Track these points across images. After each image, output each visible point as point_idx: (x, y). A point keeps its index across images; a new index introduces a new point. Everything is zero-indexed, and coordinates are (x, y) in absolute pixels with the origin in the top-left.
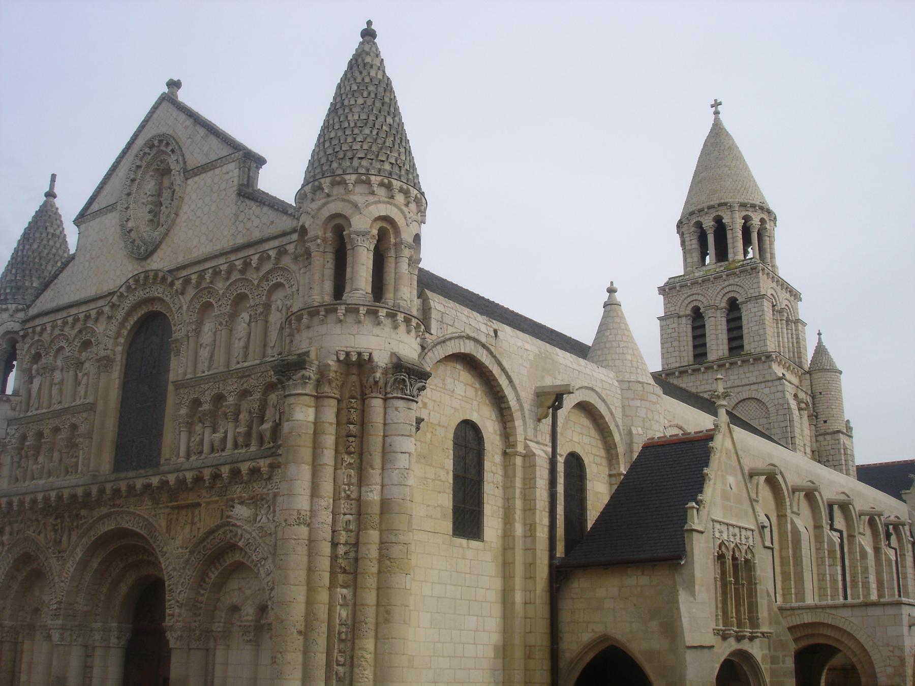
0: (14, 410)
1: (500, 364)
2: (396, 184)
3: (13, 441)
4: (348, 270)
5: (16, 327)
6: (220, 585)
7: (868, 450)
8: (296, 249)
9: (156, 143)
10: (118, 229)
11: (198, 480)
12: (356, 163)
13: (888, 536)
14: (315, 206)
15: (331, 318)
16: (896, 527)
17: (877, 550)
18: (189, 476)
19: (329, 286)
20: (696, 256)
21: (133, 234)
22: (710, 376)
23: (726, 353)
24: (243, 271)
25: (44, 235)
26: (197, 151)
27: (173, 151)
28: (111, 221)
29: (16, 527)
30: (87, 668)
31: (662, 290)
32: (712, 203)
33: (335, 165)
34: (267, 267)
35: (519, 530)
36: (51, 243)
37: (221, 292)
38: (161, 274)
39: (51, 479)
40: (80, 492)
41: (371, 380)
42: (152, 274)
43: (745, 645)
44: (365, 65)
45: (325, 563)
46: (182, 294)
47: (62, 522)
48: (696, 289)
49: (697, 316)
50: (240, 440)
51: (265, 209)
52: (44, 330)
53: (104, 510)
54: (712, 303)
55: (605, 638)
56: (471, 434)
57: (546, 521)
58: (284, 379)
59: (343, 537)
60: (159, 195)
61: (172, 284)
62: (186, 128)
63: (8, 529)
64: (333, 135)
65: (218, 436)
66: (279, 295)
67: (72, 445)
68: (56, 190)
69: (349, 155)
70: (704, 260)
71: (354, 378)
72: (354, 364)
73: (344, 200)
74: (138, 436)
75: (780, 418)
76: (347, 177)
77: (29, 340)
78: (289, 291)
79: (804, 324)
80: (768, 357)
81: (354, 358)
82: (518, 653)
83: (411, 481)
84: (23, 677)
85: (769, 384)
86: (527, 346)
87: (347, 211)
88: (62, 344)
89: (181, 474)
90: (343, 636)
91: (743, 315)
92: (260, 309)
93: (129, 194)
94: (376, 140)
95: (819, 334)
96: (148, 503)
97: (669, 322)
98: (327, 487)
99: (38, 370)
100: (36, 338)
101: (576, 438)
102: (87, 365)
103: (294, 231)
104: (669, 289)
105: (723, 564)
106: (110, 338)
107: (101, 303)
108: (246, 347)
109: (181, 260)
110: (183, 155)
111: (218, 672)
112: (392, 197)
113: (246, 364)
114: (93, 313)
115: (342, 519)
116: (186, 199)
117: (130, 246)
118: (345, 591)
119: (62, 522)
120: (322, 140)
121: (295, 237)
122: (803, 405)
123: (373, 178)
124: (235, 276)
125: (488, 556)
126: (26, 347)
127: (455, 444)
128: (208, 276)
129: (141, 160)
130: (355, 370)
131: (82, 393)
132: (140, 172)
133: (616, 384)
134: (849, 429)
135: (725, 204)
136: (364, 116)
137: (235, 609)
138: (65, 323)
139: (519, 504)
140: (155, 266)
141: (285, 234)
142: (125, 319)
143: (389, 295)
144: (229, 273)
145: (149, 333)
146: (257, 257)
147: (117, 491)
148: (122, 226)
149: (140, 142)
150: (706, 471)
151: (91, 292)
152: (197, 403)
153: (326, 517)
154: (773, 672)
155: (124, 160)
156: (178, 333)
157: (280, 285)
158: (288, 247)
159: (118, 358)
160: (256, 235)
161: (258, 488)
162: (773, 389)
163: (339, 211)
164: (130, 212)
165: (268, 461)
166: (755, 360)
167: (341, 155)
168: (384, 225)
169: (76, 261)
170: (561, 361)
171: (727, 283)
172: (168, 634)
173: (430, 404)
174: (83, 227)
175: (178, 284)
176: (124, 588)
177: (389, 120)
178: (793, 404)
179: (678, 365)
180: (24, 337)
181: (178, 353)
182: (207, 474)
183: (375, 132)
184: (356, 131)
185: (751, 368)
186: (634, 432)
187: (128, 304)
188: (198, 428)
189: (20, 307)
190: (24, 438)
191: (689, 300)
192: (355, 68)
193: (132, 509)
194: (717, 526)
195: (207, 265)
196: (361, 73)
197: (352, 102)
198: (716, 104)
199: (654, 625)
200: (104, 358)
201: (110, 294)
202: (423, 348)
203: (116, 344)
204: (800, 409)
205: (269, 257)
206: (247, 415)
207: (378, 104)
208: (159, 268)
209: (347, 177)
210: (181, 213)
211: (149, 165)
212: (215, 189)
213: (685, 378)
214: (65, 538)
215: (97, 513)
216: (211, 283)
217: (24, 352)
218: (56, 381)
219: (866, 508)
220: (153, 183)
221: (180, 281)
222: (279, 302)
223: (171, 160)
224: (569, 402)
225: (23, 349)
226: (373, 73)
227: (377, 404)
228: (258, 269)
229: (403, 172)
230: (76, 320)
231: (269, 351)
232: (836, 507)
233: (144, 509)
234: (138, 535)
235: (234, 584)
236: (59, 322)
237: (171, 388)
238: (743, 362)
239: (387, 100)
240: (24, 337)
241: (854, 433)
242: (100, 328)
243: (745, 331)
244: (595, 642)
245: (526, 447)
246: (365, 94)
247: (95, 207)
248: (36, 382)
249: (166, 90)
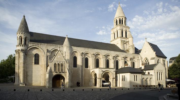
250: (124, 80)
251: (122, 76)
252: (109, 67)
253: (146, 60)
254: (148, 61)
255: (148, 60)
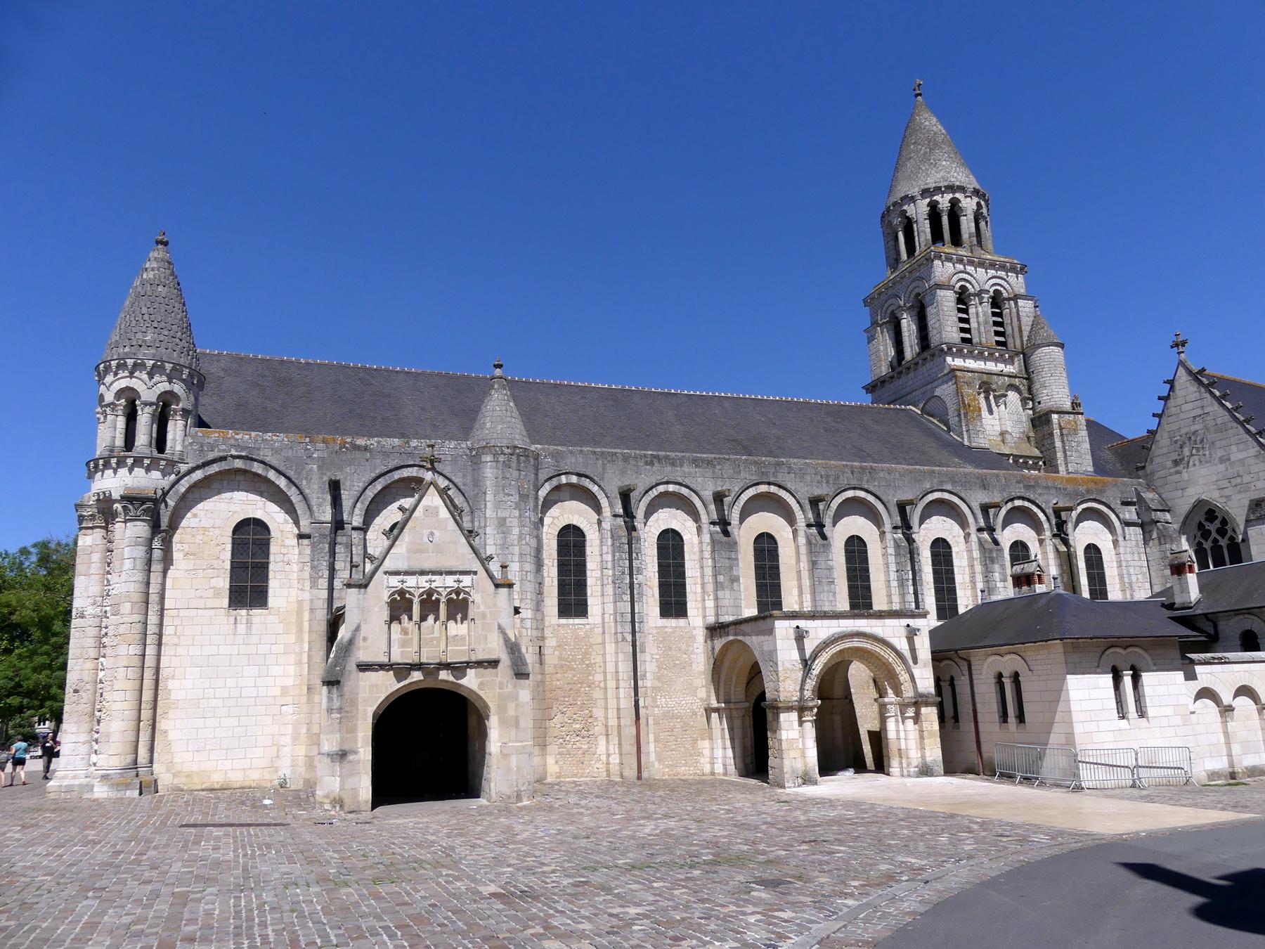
250: (1021, 718)
251: (1000, 676)
252: (870, 606)
253: (1208, 526)
254: (1222, 532)
255: (1224, 522)
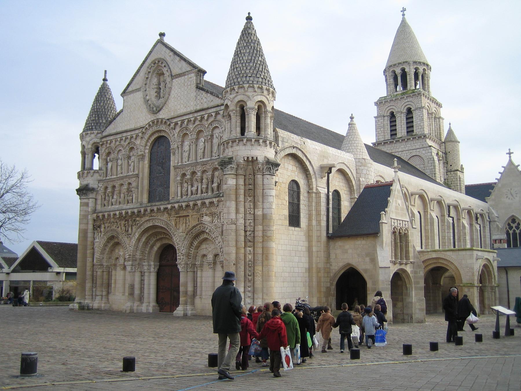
0: (101, 176)
1: (306, 156)
2: (264, 87)
3: (102, 189)
4: (246, 123)
5: (98, 140)
6: (198, 247)
7: (471, 178)
8: (224, 113)
9: (157, 62)
10: (142, 99)
11: (188, 206)
12: (248, 79)
13: (477, 219)
14: (232, 96)
15: (241, 143)
16: (481, 215)
17: (471, 225)
18: (184, 204)
19: (239, 129)
20: (393, 86)
21: (149, 102)
22: (398, 144)
23: (406, 134)
24: (201, 121)
25: (105, 99)
26: (177, 67)
27: (165, 66)
28: (139, 95)
29: (107, 225)
30: (142, 281)
31: (376, 104)
32: (400, 61)
33: (239, 80)
34: (211, 119)
35: (314, 223)
36: (108, 102)
37: (192, 129)
38: (164, 121)
39: (121, 205)
40: (136, 211)
41: (257, 167)
42: (160, 120)
43: (403, 267)
44: (249, 34)
45: (242, 238)
46: (174, 129)
47: (128, 223)
48: (392, 103)
49: (392, 115)
50: (204, 190)
51: (209, 95)
52: (111, 142)
53: (147, 218)
54: (399, 110)
55: (348, 264)
56: (295, 186)
57: (325, 218)
58: (223, 168)
59: (248, 228)
60: (159, 84)
61: (169, 125)
62: (170, 56)
63: (103, 226)
64: (237, 66)
65: (194, 188)
66: (217, 131)
67: (129, 191)
68: (107, 78)
69: (245, 75)
70: (396, 88)
71: (250, 167)
72: (250, 161)
73: (243, 95)
74: (158, 188)
75: (430, 165)
76: (245, 85)
77: (104, 146)
78: (221, 130)
79: (443, 119)
80: (425, 136)
81: (250, 159)
82: (314, 270)
83: (274, 207)
84: (113, 285)
85: (425, 149)
86: (317, 148)
87: (245, 99)
88: (120, 149)
89: (180, 204)
90: (250, 265)
91: (414, 116)
92: (209, 137)
93: (146, 84)
94: (255, 68)
95: (450, 124)
96: (166, 215)
97: (379, 119)
98: (242, 210)
99: (110, 159)
100: (108, 146)
101: (337, 184)
102: (133, 158)
103: (222, 105)
104: (380, 103)
105: (395, 236)
106: (143, 146)
107: (137, 132)
108: (204, 152)
109: (172, 115)
110: (170, 68)
111: (199, 280)
112: (263, 92)
113: (204, 160)
114: (134, 136)
115: (248, 222)
116: (173, 88)
117: (149, 107)
118: (250, 249)
119: (128, 223)
120: (233, 68)
121: (223, 107)
122: (441, 158)
123: (255, 85)
124: (197, 123)
125: (302, 234)
126: (103, 149)
127: (289, 190)
128: (185, 123)
129: (150, 69)
130: (251, 164)
131: (132, 169)
132: (150, 75)
133: (354, 160)
134: (462, 168)
135: (406, 62)
136: (250, 58)
137: (204, 256)
138: (121, 140)
139: (314, 213)
140: (161, 117)
141: (218, 106)
142: (149, 139)
143: (262, 133)
144: (195, 121)
145: (160, 145)
146: (207, 115)
147: (152, 211)
148: (144, 98)
149: (149, 61)
150: (389, 199)
151: (132, 127)
152: (184, 175)
153: (242, 221)
154: (415, 277)
155: (142, 68)
156: (173, 146)
157: (216, 127)
158: (220, 112)
159: (147, 155)
160: (205, 106)
161: (213, 209)
162: (427, 151)
163: (242, 99)
164: (147, 92)
165: (217, 199)
166: (419, 137)
167: (241, 75)
168: (260, 104)
169: (124, 112)
170: (331, 152)
171: (406, 101)
172: (179, 266)
173: (279, 174)
174: (125, 97)
175: (172, 125)
176: (156, 248)
177: (260, 59)
178: (436, 158)
179: (383, 139)
180: (102, 145)
181: (174, 154)
182: (191, 204)
183: (255, 65)
184: (247, 64)
185: (417, 141)
186: (361, 179)
187: (150, 132)
188: (185, 185)
189: (99, 132)
190: (106, 188)
191: (389, 108)
192: (245, 35)
193: (159, 217)
194: (393, 220)
195: (184, 118)
196: (247, 38)
197: (245, 51)
198: (404, 10)
199: (367, 259)
200: (140, 155)
201: (141, 128)
202: (276, 153)
203: (145, 149)
204: (439, 160)
205: (212, 115)
206: (206, 180)
207: (255, 52)
208: (164, 117)
209: (245, 85)
210: (171, 94)
211: (154, 71)
212: (186, 85)
213: (387, 146)
214: (130, 229)
215: (144, 219)
216: (187, 125)
217: (103, 151)
218: (119, 164)
219: (467, 207)
220: (156, 79)
221: (173, 124)
222: (217, 134)
223: (165, 70)
224: (334, 170)
225: (102, 150)
226: (252, 38)
227: (259, 177)
228: (207, 120)
229: (267, 82)
230: (126, 138)
231: (214, 154)
232: (451, 207)
233: (165, 217)
234: (162, 228)
235: (204, 246)
236: (119, 139)
237: (172, 168)
238: (413, 138)
239: (258, 49)
240: (102, 145)
241: (464, 171)
242: (138, 142)
243: (414, 124)
244: (345, 266)
245: (317, 189)
246: (250, 47)
247: (130, 89)
248: (110, 165)
249: (159, 38)
253: (512, 224)
255: (519, 224)
